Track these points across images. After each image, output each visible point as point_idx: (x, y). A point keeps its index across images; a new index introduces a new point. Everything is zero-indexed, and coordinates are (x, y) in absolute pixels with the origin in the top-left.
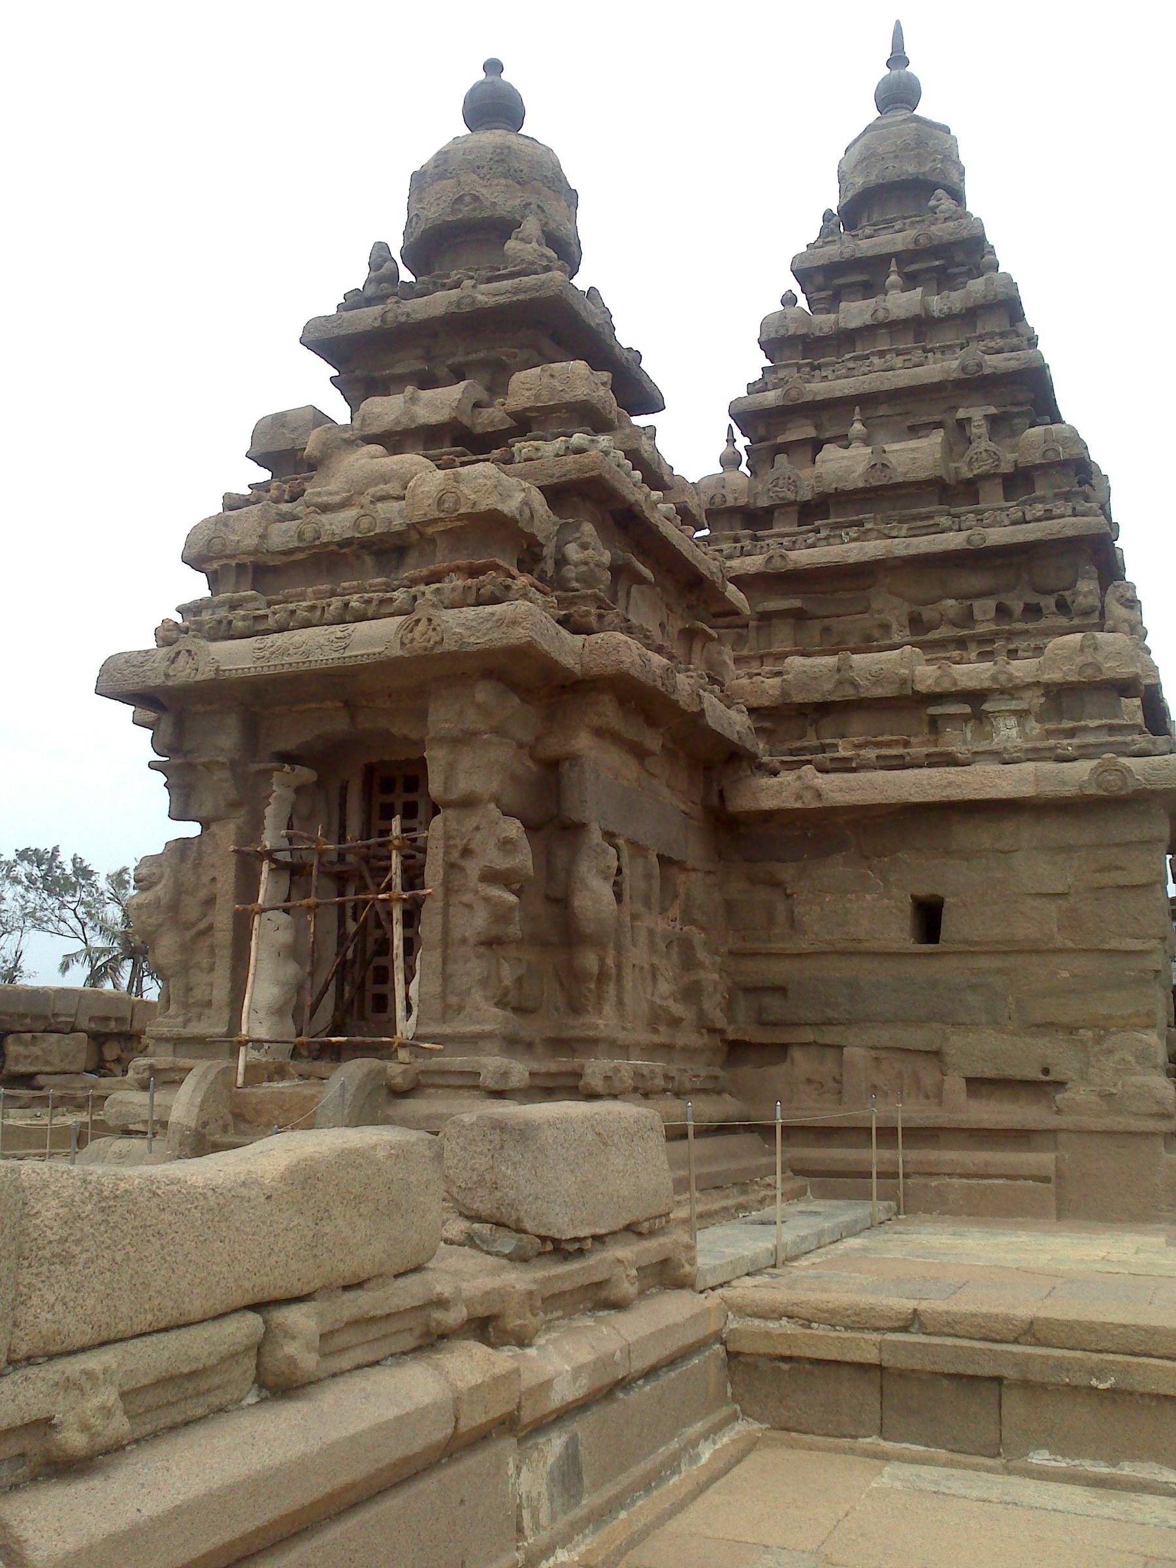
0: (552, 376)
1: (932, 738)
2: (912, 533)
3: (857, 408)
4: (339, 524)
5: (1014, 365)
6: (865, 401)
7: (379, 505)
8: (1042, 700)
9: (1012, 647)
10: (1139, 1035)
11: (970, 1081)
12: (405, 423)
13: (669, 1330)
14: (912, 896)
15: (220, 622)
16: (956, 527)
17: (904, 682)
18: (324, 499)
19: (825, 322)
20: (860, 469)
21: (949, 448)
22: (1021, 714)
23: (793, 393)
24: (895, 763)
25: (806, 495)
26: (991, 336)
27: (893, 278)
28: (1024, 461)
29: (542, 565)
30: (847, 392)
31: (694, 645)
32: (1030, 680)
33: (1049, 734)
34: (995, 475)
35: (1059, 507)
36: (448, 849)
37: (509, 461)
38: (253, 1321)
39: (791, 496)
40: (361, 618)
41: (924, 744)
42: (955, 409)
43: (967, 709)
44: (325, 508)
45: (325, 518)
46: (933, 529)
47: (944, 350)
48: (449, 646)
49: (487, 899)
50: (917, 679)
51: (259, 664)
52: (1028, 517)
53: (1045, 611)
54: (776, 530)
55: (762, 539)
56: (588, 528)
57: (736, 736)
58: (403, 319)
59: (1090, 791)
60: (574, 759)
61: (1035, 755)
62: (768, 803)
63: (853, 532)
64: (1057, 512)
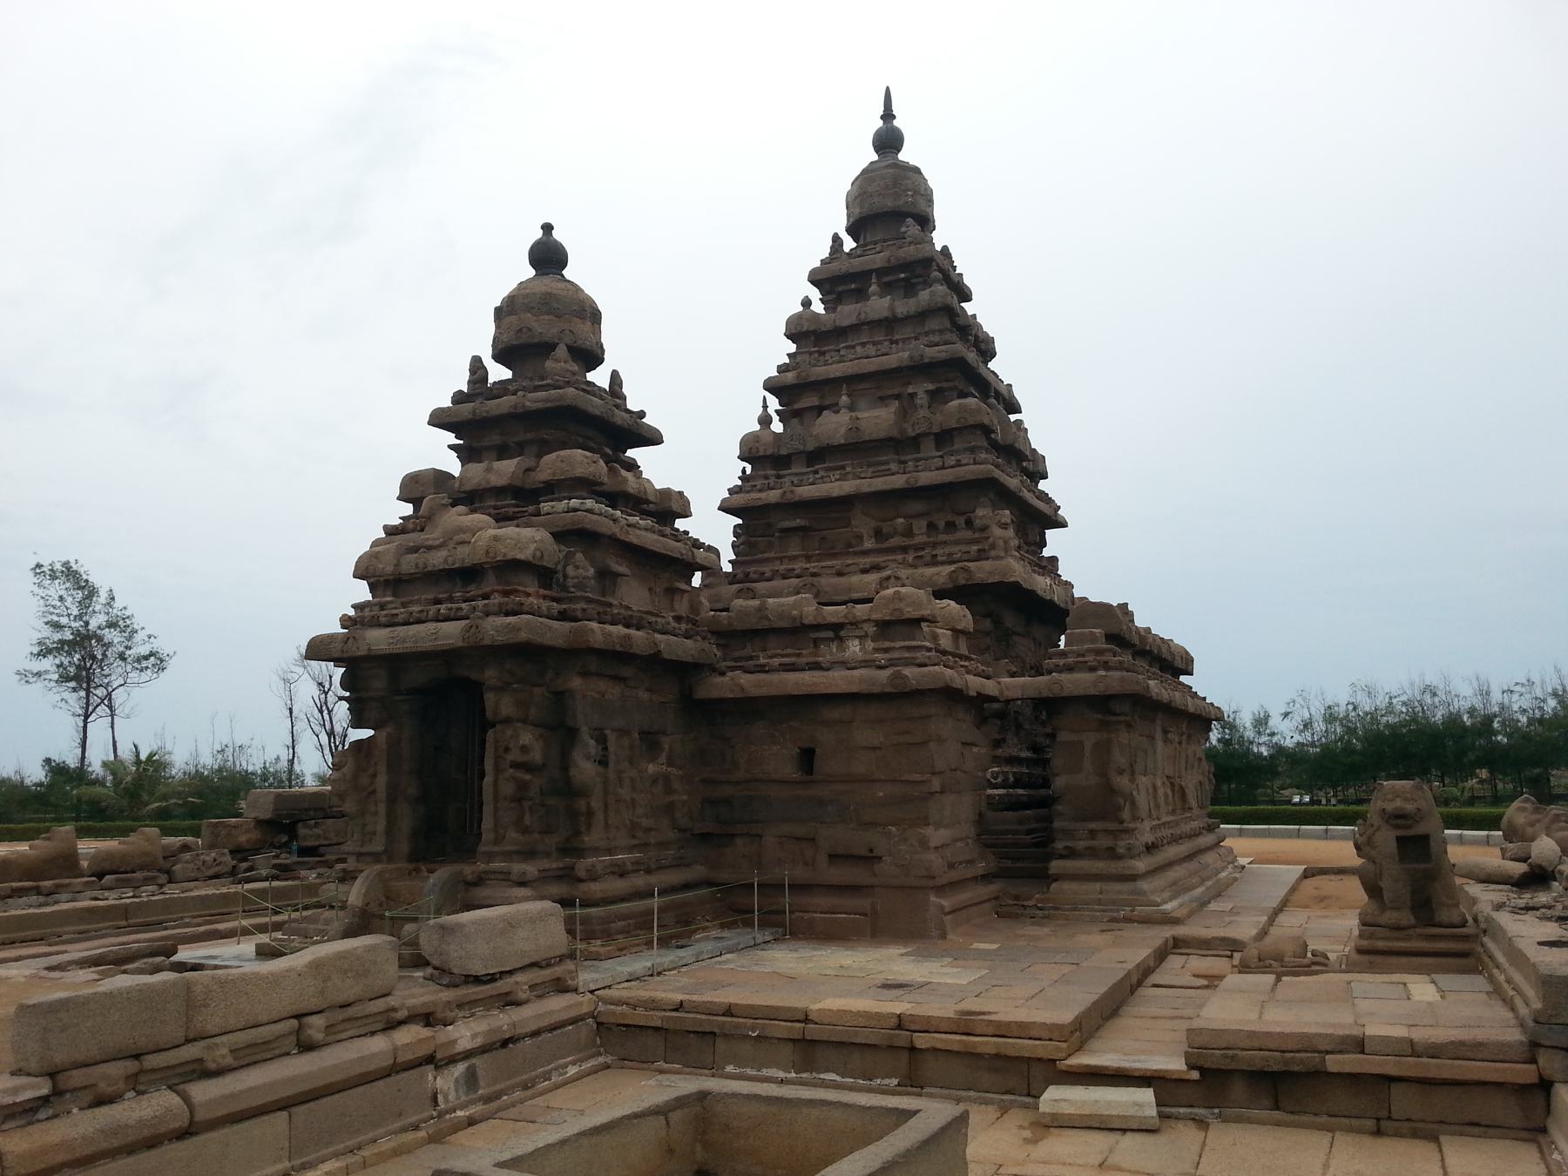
0: (562, 461)
1: (814, 650)
2: (875, 474)
3: (844, 386)
4: (437, 559)
5: (943, 356)
6: (851, 380)
7: (459, 549)
8: (875, 629)
9: (934, 553)
10: (922, 831)
11: (830, 855)
12: (484, 485)
13: (551, 1013)
14: (799, 748)
15: (373, 617)
16: (902, 471)
17: (794, 619)
18: (430, 543)
20: (843, 430)
21: (903, 414)
23: (804, 374)
24: (788, 667)
25: (811, 446)
26: (933, 332)
27: (874, 288)
29: (557, 575)
30: (838, 374)
31: (675, 598)
33: (876, 650)
34: (929, 433)
35: (965, 458)
36: (496, 750)
37: (539, 514)
38: (295, 1022)
39: (801, 448)
40: (447, 619)
42: (910, 383)
43: (830, 634)
44: (430, 548)
46: (888, 473)
47: (904, 340)
48: (487, 642)
50: (804, 617)
51: (391, 647)
52: (946, 465)
53: (958, 527)
54: (793, 471)
55: (784, 476)
56: (579, 556)
57: (690, 657)
58: (485, 414)
59: (888, 689)
61: (865, 664)
62: (715, 694)
64: (964, 462)
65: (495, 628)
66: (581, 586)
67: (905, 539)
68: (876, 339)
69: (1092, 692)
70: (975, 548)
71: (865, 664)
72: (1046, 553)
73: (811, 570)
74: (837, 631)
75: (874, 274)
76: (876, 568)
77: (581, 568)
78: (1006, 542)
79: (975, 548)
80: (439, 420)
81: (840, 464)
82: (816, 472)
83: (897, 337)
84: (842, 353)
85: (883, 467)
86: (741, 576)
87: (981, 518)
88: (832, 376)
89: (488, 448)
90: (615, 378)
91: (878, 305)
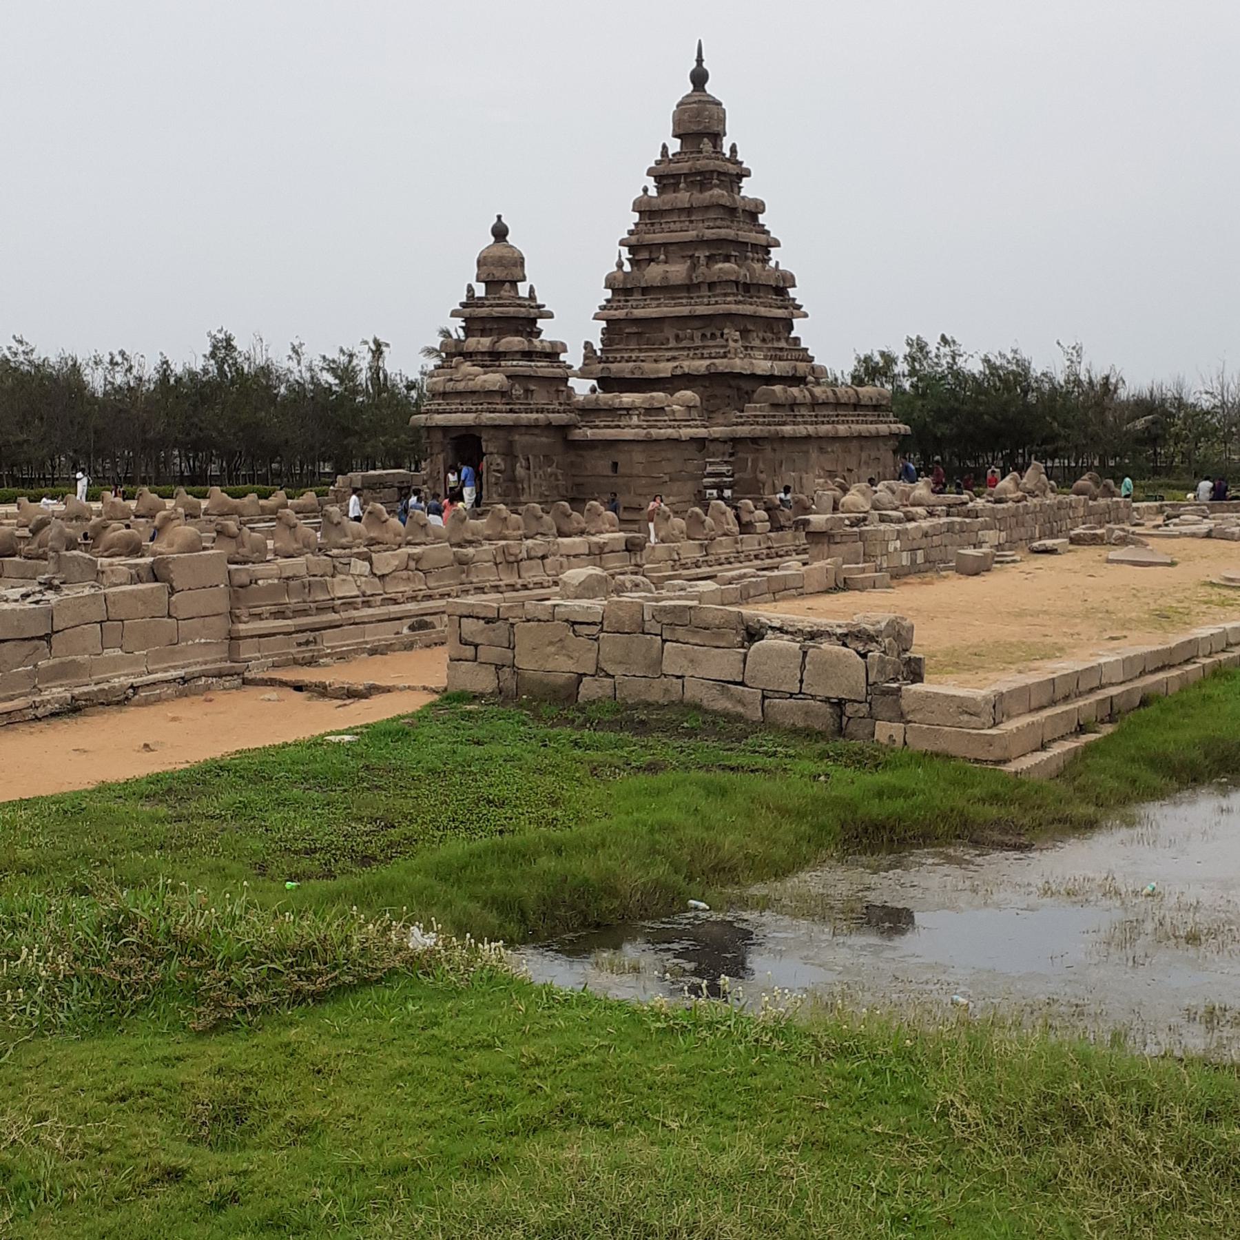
4: (461, 386)
19: (658, 204)
21: (694, 267)
22: (638, 415)
27: (682, 186)
37: (500, 366)
43: (625, 412)
62: (577, 438)
65: (487, 418)
68: (682, 219)
72: (793, 334)
76: (674, 358)
77: (518, 391)
80: (454, 314)
82: (645, 300)
83: (693, 218)
86: (604, 359)
90: (532, 290)
91: (683, 197)
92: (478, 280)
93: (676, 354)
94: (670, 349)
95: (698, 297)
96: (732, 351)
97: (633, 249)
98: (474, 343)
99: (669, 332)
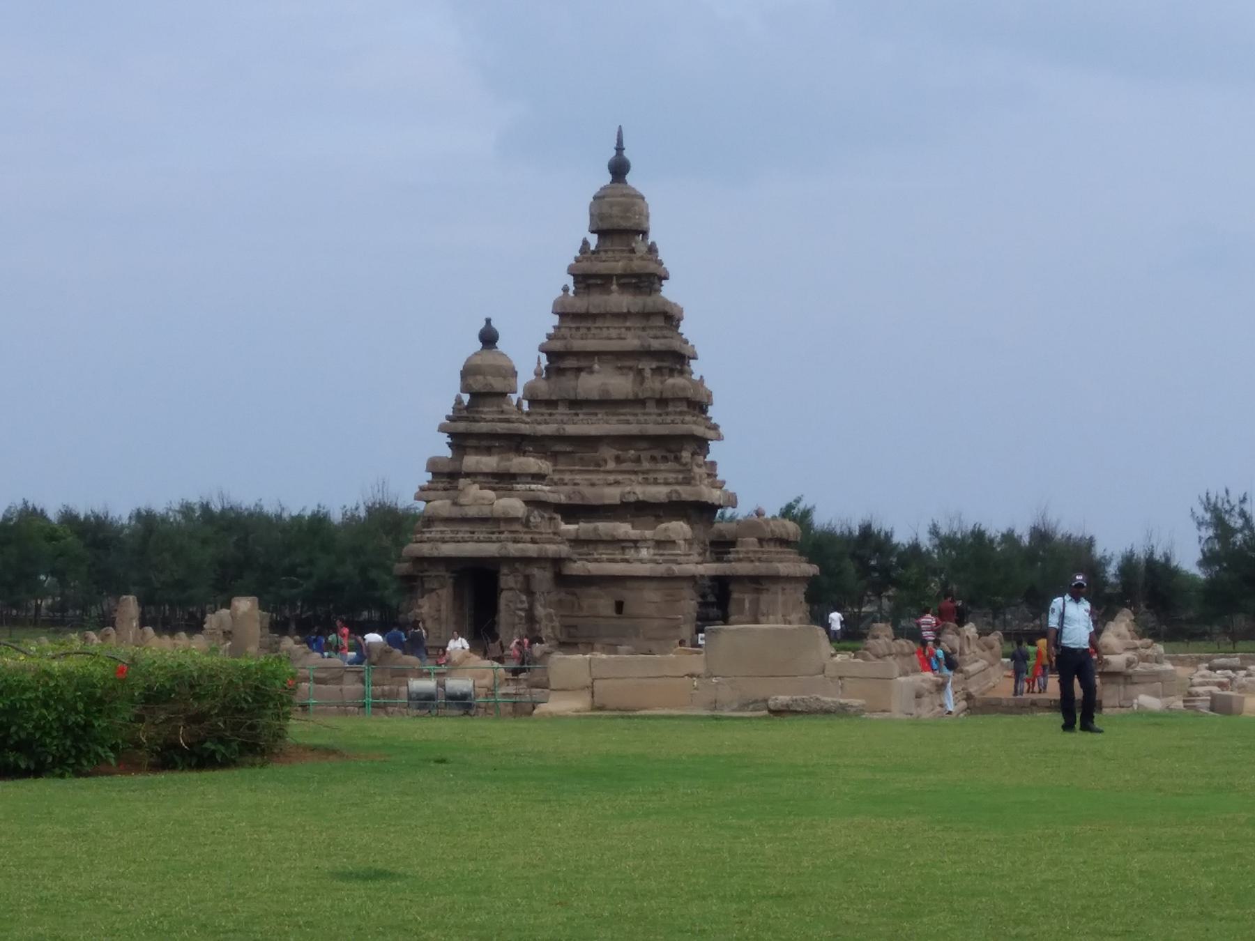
3: (596, 358)
4: (472, 512)
5: (663, 348)
9: (655, 476)
12: (479, 470)
22: (648, 548)
26: (655, 327)
27: (614, 287)
28: (665, 396)
32: (651, 538)
33: (655, 555)
35: (678, 418)
37: (511, 490)
41: (620, 554)
43: (632, 545)
45: (467, 508)
48: (511, 555)
49: (518, 616)
60: (534, 575)
61: (651, 561)
62: (574, 573)
63: (594, 418)
64: (676, 422)
65: (513, 549)
66: (536, 527)
67: (634, 464)
69: (752, 573)
70: (681, 476)
71: (651, 561)
72: (709, 458)
73: (576, 481)
74: (635, 543)
75: (614, 278)
76: (617, 483)
77: (536, 518)
78: (701, 476)
79: (681, 476)
80: (442, 429)
81: (592, 411)
83: (628, 324)
84: (594, 331)
85: (622, 417)
87: (685, 458)
88: (588, 349)
89: (471, 447)
92: (465, 389)
93: (620, 477)
94: (610, 472)
95: (644, 414)
96: (698, 477)
97: (552, 355)
98: (472, 461)
99: (608, 452)
